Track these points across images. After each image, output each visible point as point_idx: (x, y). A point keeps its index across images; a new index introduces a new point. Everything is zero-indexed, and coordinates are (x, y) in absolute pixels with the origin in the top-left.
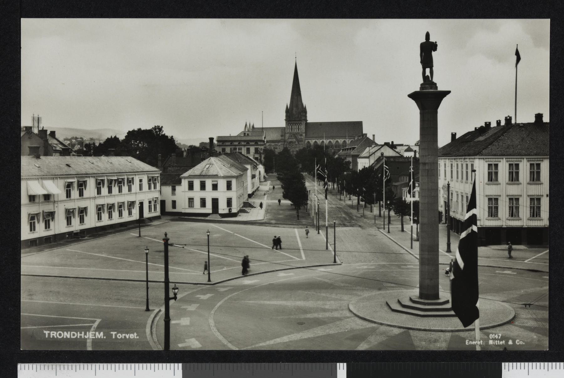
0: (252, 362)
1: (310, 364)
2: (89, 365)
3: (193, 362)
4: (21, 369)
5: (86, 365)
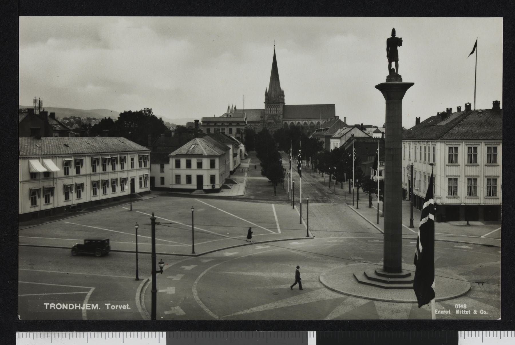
0: (230, 330)
1: (283, 332)
2: (82, 333)
3: (176, 331)
4: (19, 337)
5: (78, 333)
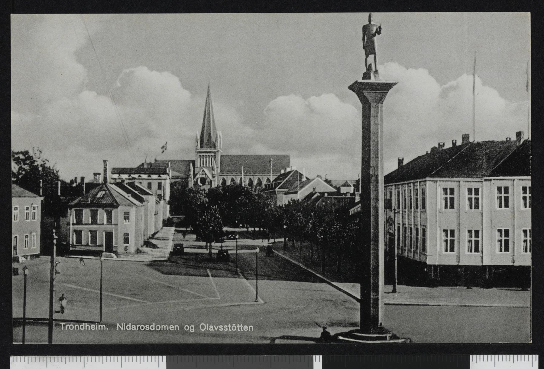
1: (288, 356)
2: (78, 357)
3: (176, 355)
4: (13, 361)
5: (75, 357)
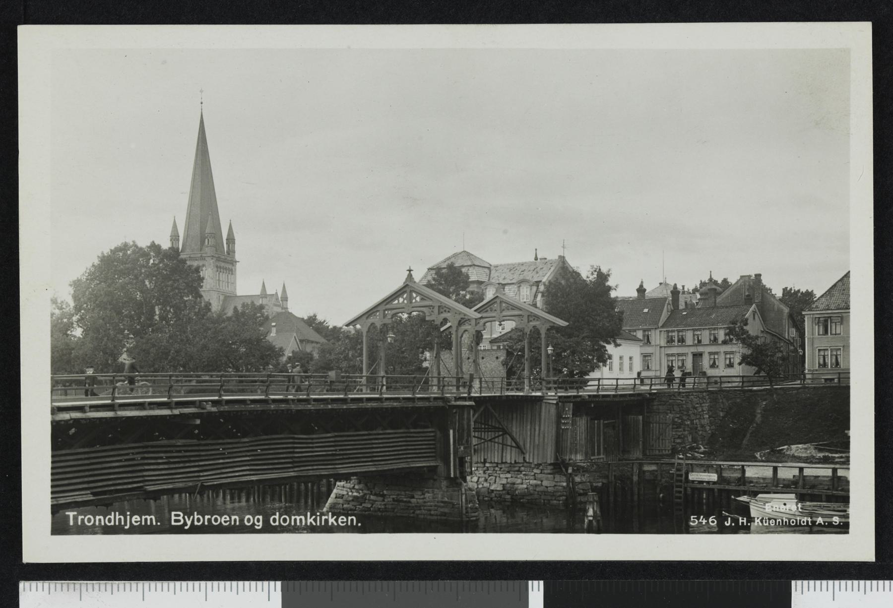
0: (393, 579)
1: (485, 582)
2: (134, 583)
4: (24, 591)
5: (127, 583)
